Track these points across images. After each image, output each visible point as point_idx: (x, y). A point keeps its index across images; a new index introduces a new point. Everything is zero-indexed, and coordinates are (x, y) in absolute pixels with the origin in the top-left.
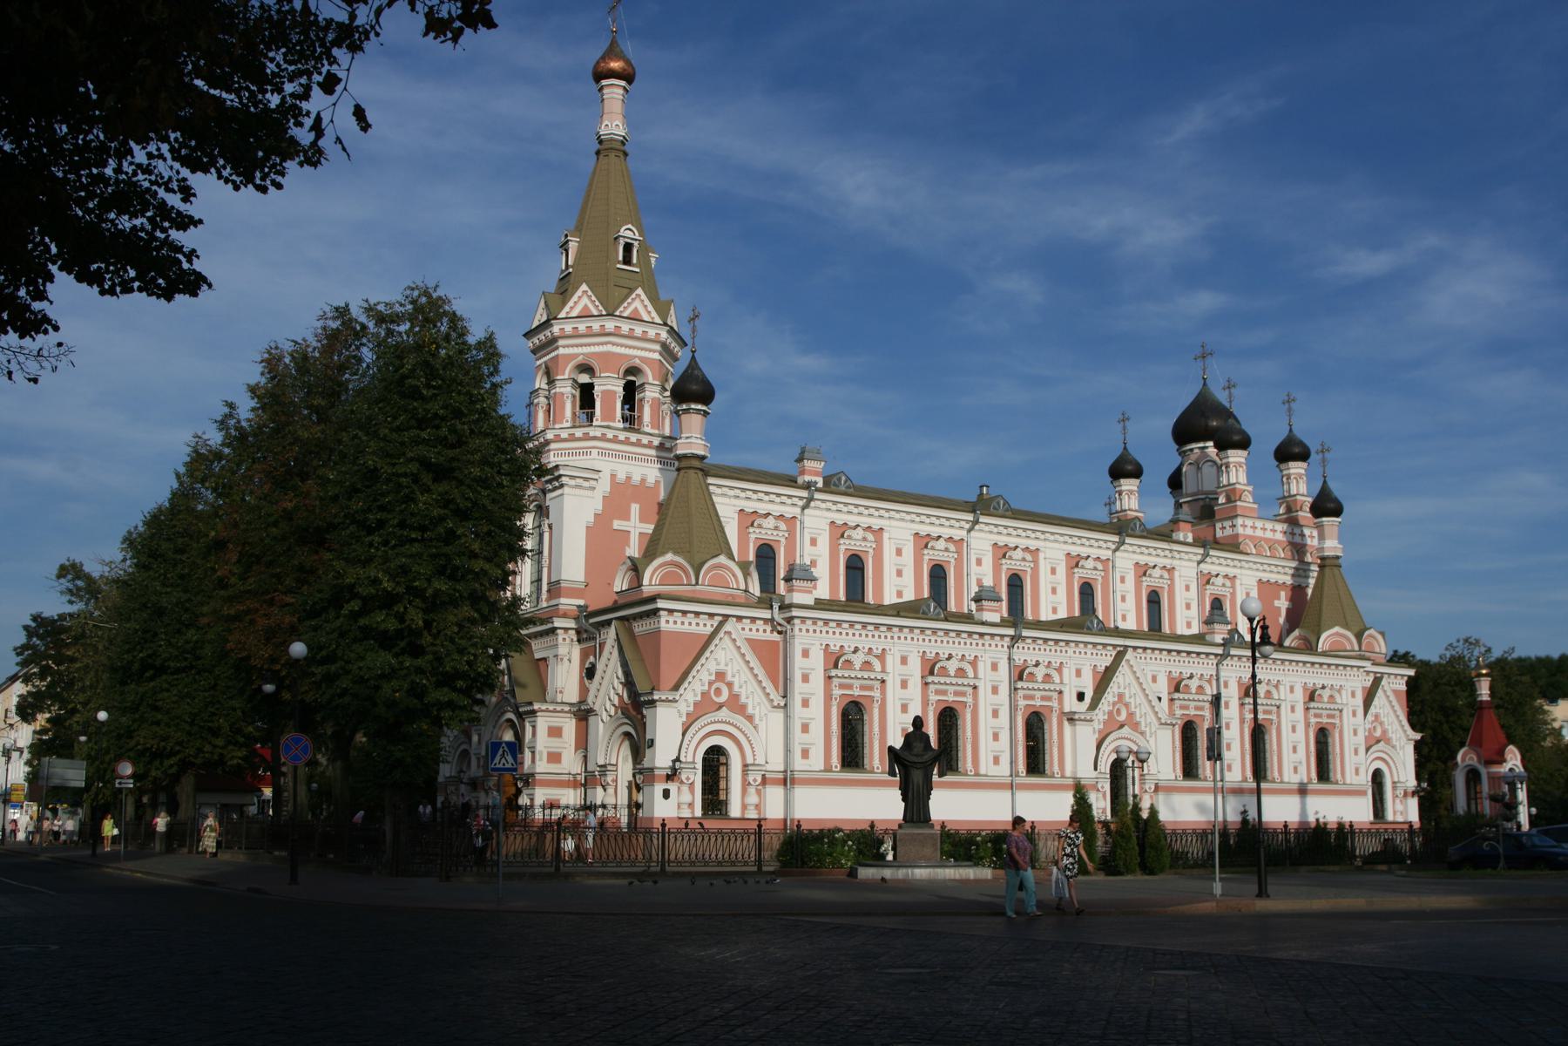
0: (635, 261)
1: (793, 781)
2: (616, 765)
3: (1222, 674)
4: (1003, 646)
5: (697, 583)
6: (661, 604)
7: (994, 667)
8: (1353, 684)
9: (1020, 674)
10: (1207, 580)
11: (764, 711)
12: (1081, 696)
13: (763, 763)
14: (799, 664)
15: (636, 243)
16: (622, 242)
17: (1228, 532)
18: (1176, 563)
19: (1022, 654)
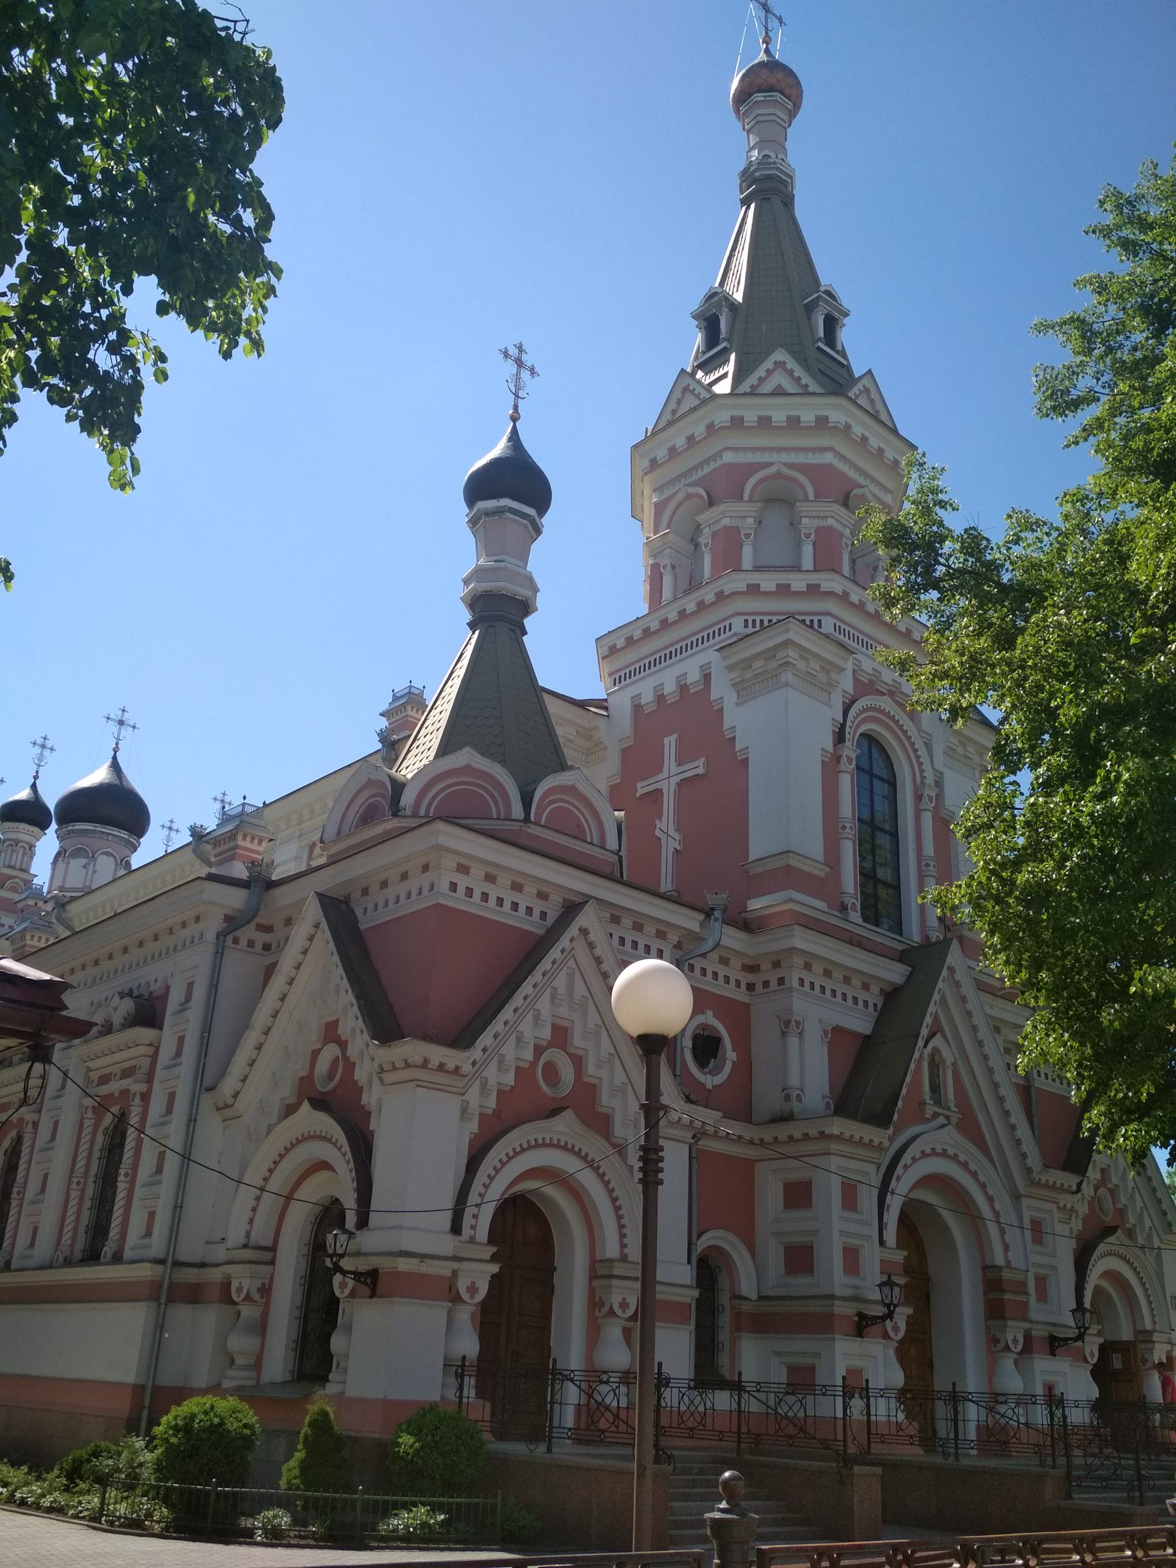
2: (273, 1249)
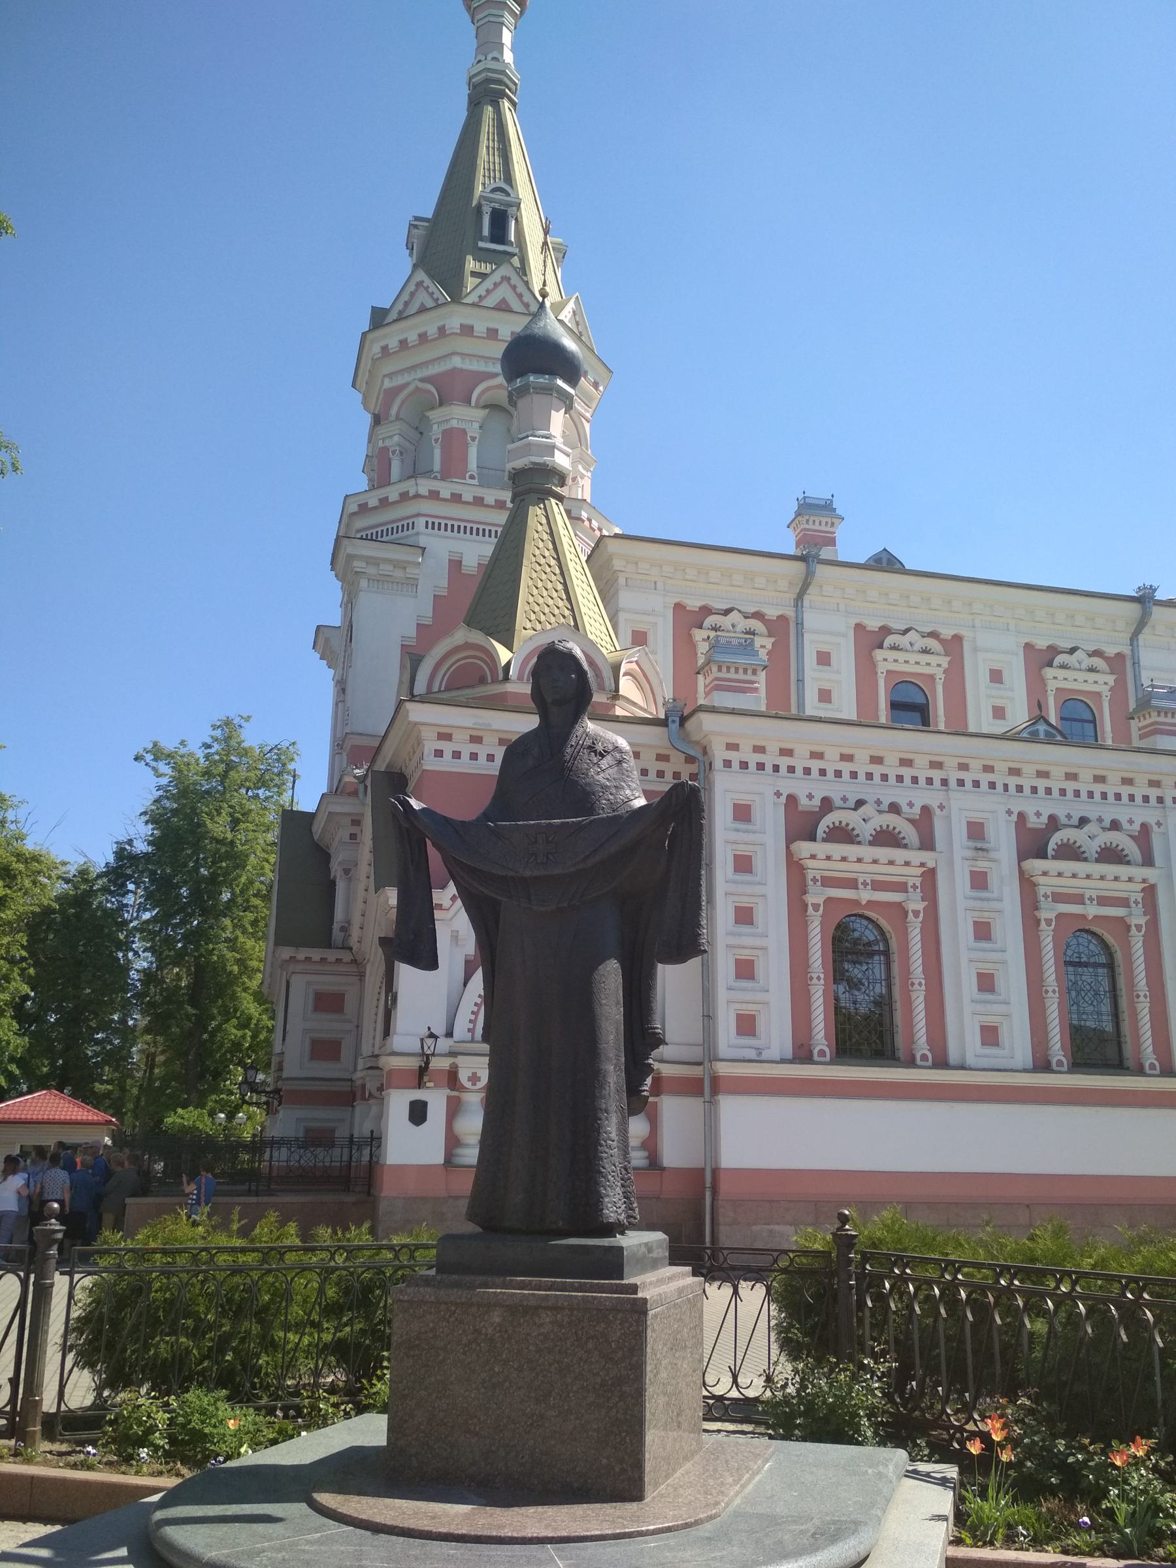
1: (717, 1086)
5: (506, 678)
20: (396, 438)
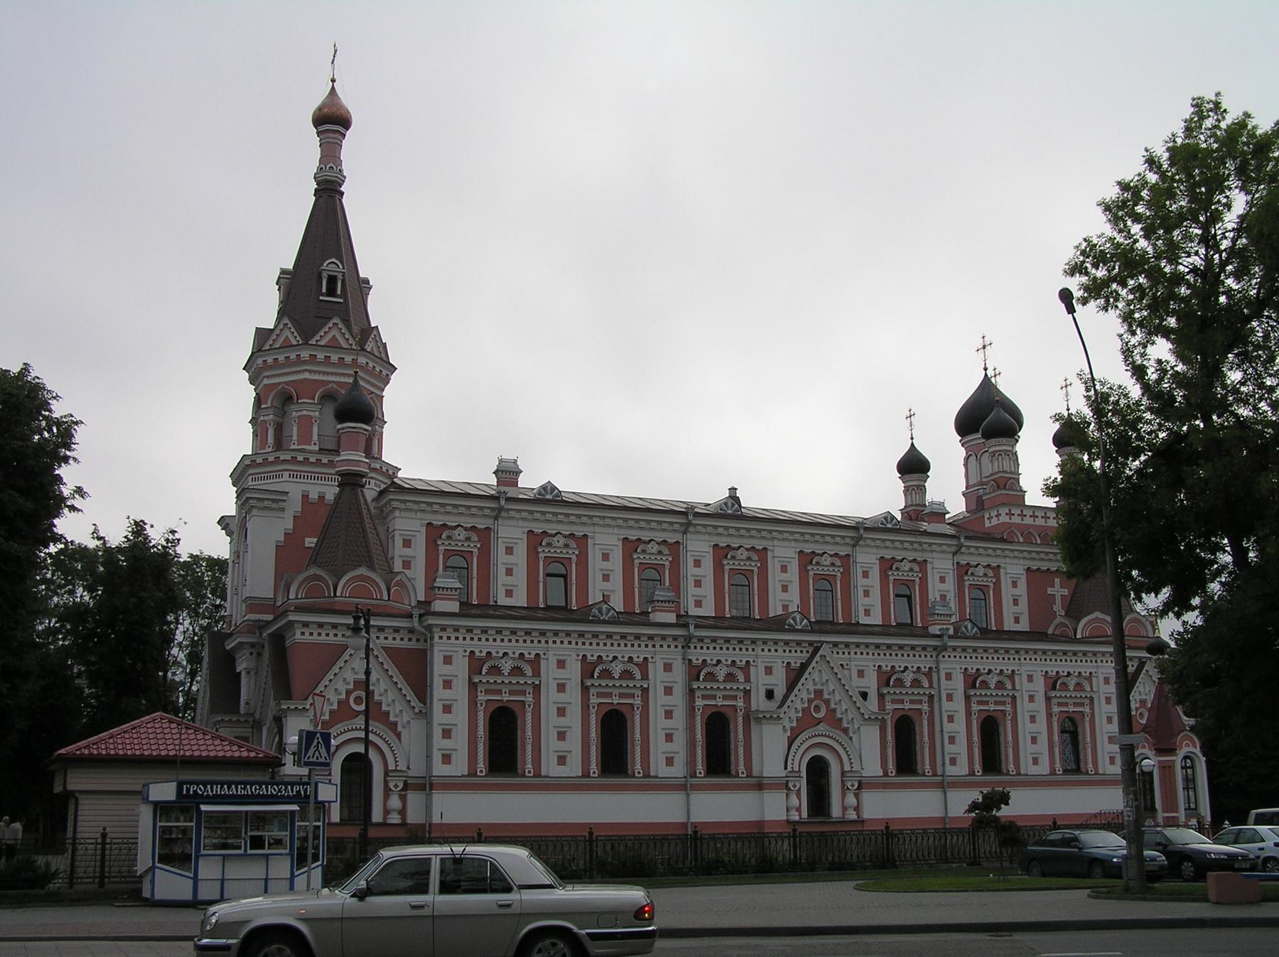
0: (339, 293)
3: (942, 666)
4: (676, 647)
6: (292, 617)
7: (668, 667)
8: (1104, 671)
9: (694, 672)
10: (963, 571)
11: (406, 717)
12: (770, 695)
13: (405, 769)
14: (439, 670)
15: (340, 276)
16: (325, 275)
17: (995, 521)
18: (927, 556)
19: (697, 656)
20: (271, 417)
